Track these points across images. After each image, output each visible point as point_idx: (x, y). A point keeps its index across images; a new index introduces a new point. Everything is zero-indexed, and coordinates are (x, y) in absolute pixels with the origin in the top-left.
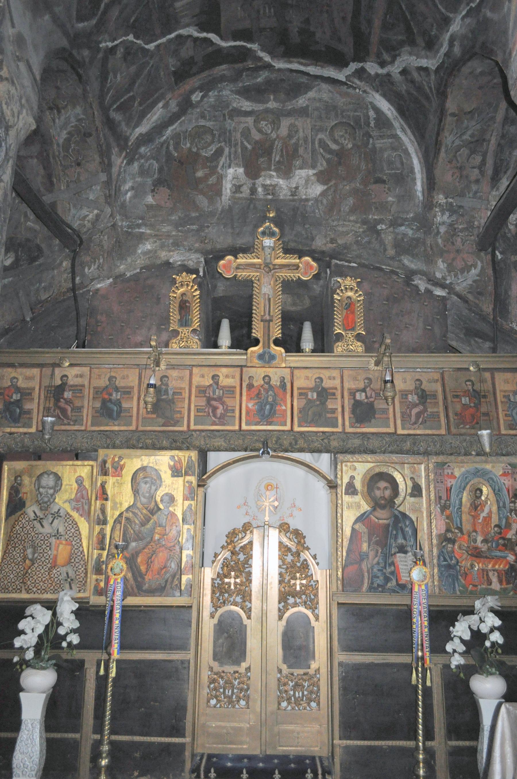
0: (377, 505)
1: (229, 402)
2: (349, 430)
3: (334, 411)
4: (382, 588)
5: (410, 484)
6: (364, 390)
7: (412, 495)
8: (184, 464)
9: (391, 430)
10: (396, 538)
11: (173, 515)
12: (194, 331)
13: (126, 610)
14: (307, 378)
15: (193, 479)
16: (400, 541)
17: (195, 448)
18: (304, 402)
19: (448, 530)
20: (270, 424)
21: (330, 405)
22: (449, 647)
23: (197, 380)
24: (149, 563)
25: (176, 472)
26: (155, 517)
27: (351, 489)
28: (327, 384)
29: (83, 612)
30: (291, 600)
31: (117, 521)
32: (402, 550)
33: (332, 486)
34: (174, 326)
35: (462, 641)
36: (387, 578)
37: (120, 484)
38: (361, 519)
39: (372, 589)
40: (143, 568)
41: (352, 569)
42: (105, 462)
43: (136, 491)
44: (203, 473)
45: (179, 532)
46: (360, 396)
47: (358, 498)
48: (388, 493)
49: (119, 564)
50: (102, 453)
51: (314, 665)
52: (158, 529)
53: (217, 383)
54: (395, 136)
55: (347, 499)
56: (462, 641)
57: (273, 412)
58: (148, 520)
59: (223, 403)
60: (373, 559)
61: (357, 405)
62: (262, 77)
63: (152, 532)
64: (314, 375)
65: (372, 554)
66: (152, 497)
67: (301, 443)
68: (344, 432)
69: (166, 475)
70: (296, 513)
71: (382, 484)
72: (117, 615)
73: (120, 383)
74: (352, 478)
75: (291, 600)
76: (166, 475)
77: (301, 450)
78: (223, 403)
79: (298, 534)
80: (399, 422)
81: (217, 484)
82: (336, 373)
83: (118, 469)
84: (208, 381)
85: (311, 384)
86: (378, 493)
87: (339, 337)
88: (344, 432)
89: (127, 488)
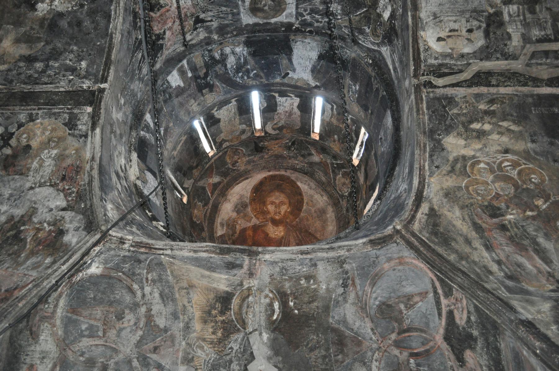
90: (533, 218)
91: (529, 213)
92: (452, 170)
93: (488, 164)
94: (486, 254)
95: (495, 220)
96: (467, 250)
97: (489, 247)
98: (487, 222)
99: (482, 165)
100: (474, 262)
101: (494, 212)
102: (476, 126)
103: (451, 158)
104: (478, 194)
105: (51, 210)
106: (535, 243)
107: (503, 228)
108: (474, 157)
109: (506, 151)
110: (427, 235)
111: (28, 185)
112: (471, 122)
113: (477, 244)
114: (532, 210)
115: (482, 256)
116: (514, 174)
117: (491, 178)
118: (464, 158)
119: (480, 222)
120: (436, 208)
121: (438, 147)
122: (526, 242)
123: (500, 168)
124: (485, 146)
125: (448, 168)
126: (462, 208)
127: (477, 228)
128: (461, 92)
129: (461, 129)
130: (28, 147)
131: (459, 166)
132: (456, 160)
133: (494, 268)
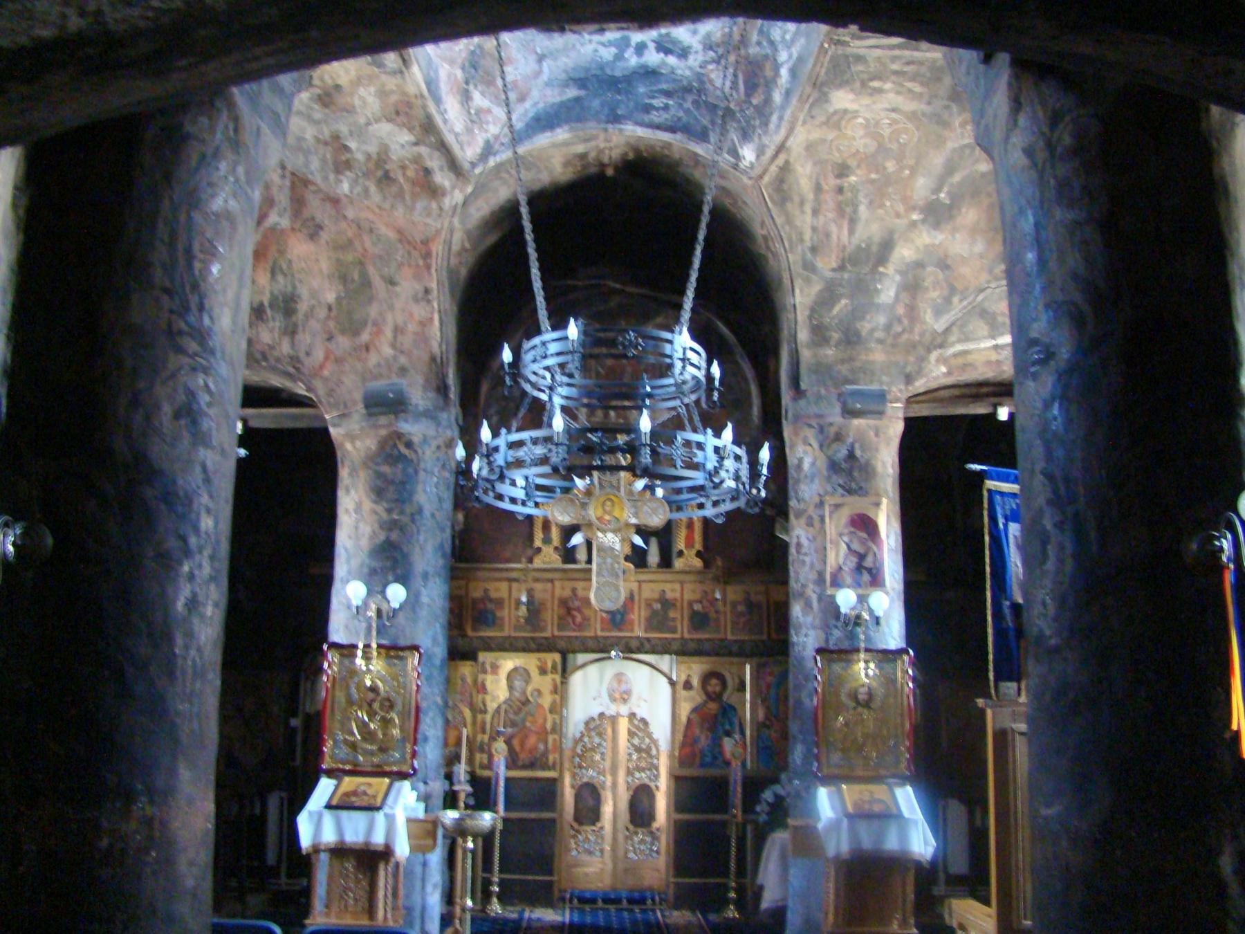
0: (710, 697)
2: (686, 636)
3: (674, 620)
4: (711, 765)
5: (737, 681)
7: (739, 690)
8: (549, 665)
9: (722, 636)
10: (723, 725)
11: (540, 706)
12: (556, 548)
13: (507, 780)
14: (652, 590)
15: (558, 678)
16: (727, 727)
17: (559, 651)
19: (767, 718)
20: (620, 630)
21: (672, 614)
22: (758, 808)
23: (558, 592)
24: (522, 744)
25: (543, 671)
26: (526, 709)
27: (688, 685)
28: (669, 595)
29: (474, 780)
31: (498, 710)
32: (728, 734)
33: (672, 683)
34: (538, 543)
35: (768, 804)
37: (497, 681)
38: (695, 710)
39: (702, 765)
40: (517, 748)
41: (687, 750)
42: (483, 663)
43: (511, 688)
44: (565, 671)
45: (545, 720)
46: (697, 607)
47: (692, 693)
48: (718, 689)
49: (500, 747)
50: (482, 656)
51: (655, 825)
52: (530, 718)
54: (736, 363)
55: (683, 693)
56: (768, 804)
57: (622, 620)
58: (520, 710)
60: (704, 741)
62: (613, 303)
63: (524, 721)
64: (658, 587)
65: (703, 739)
66: (524, 693)
67: (647, 646)
68: (682, 638)
69: (534, 673)
70: (642, 704)
71: (714, 681)
73: (493, 595)
77: (646, 653)
79: (644, 721)
81: (577, 679)
82: (677, 586)
83: (495, 668)
84: (567, 593)
85: (656, 596)
86: (710, 689)
87: (681, 553)
88: (682, 638)
89: (504, 682)
90: (872, 182)
91: (873, 176)
92: (826, 123)
93: (866, 119)
94: (808, 218)
95: (838, 181)
96: (797, 213)
97: (815, 212)
98: (831, 182)
99: (860, 120)
100: (796, 227)
101: (842, 171)
102: (875, 84)
103: (831, 110)
104: (839, 150)
105: (403, 146)
106: (855, 211)
107: (840, 190)
108: (857, 111)
109: (894, 110)
110: (770, 191)
111: (362, 121)
112: (871, 80)
113: (808, 209)
114: (877, 172)
115: (805, 221)
116: (886, 132)
117: (861, 132)
118: (845, 111)
119: (823, 183)
120: (792, 160)
121: (824, 98)
122: (848, 210)
123: (877, 124)
124: (874, 103)
125: (823, 119)
126: (815, 164)
127: (818, 189)
128: (878, 52)
129: (857, 85)
130: (338, 87)
131: (836, 118)
132: (836, 112)
133: (808, 235)
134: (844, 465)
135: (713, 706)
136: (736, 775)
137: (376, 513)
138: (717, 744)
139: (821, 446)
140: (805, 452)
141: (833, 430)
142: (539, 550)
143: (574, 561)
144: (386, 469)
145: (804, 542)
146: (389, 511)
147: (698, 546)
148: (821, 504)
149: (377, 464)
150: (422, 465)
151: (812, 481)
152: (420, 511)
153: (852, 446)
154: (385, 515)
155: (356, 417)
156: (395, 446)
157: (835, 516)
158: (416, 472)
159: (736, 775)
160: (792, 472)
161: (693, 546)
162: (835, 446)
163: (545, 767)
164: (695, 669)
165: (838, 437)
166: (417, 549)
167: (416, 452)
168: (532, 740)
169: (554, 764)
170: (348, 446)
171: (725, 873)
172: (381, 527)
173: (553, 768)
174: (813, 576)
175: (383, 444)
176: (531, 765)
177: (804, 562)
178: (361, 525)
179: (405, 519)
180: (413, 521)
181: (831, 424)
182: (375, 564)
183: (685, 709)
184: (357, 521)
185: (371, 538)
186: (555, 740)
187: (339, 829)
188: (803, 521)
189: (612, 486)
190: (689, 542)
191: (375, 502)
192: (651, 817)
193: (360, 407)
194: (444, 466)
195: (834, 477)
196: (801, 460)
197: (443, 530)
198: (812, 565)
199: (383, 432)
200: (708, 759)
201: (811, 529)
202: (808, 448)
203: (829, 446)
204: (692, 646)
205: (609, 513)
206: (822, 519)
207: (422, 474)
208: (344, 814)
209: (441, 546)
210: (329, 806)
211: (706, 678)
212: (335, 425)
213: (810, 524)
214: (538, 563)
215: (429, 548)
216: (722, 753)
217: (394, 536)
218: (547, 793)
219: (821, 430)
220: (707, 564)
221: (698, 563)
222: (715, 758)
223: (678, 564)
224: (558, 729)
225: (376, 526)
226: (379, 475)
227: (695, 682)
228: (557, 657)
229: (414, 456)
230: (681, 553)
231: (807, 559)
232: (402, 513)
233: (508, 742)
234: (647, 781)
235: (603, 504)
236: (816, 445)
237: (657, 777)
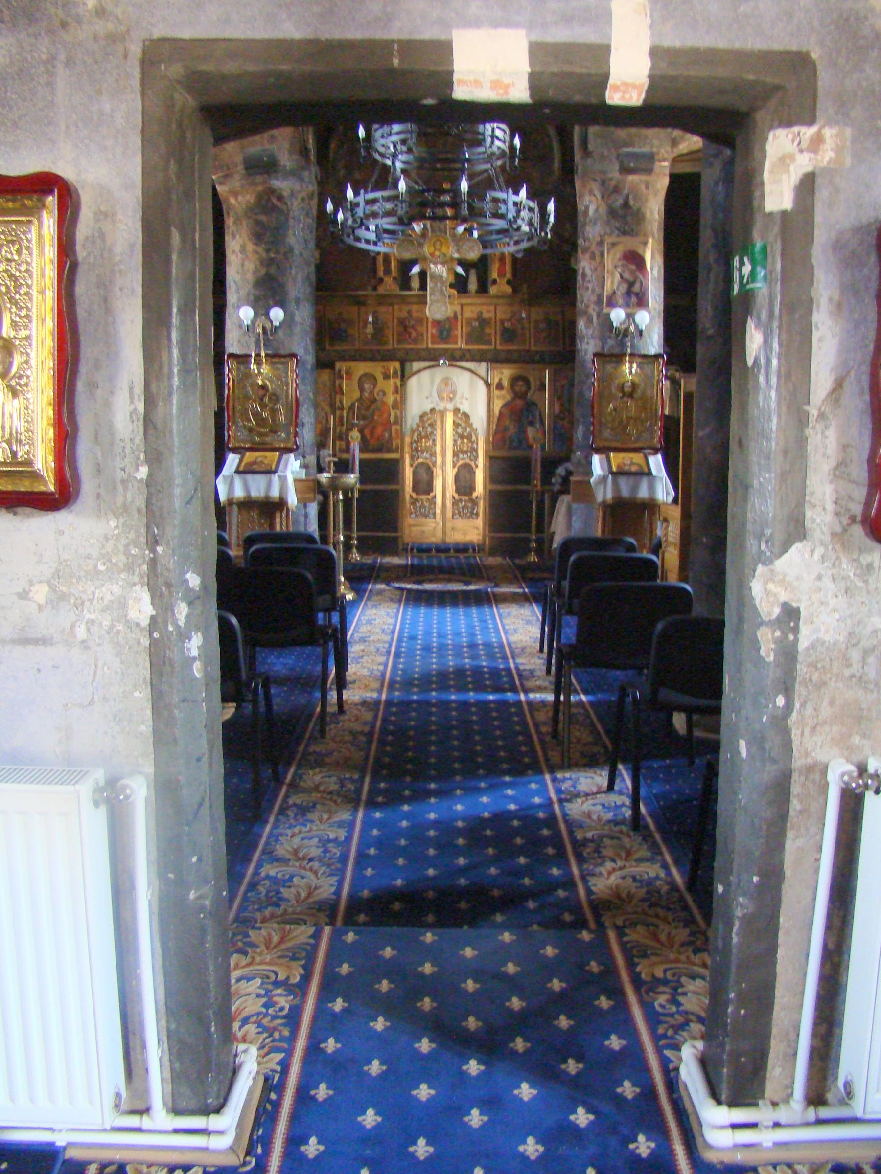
0: (516, 395)
1: (419, 329)
2: (499, 347)
3: (489, 334)
4: (515, 448)
5: (538, 383)
6: (510, 320)
9: (527, 348)
11: (384, 403)
12: (394, 278)
13: (361, 461)
17: (398, 360)
18: (469, 329)
19: (561, 412)
20: (447, 343)
21: (487, 331)
22: (553, 480)
23: (397, 314)
27: (500, 386)
28: (486, 315)
30: (461, 456)
31: (351, 408)
32: (531, 423)
33: (488, 385)
34: (381, 274)
36: (521, 441)
38: (505, 406)
40: (368, 437)
41: (499, 436)
42: (340, 371)
43: (362, 390)
44: (404, 377)
46: (507, 325)
47: (504, 392)
48: (523, 389)
49: (355, 435)
50: (338, 365)
51: (475, 495)
53: (411, 316)
55: (497, 393)
57: (448, 335)
58: (370, 407)
59: (416, 330)
60: (512, 430)
61: (505, 330)
63: (373, 414)
64: (476, 309)
65: (512, 427)
66: (371, 393)
67: (468, 356)
69: (380, 378)
70: (464, 401)
71: (520, 383)
72: (357, 463)
73: (345, 316)
74: (501, 380)
75: (461, 456)
76: (380, 378)
77: (467, 361)
78: (416, 330)
79: (466, 415)
80: (532, 341)
81: (413, 383)
82: (492, 308)
84: (404, 314)
85: (475, 316)
86: (517, 389)
87: (495, 282)
134: (620, 212)
135: (519, 403)
136: (537, 456)
137: (257, 253)
138: (522, 432)
139: (603, 197)
140: (590, 201)
141: (613, 183)
142: (381, 280)
143: (409, 289)
144: (263, 218)
145: (588, 272)
146: (268, 251)
147: (509, 276)
148: (601, 243)
149: (256, 214)
150: (291, 214)
151: (595, 224)
152: (291, 249)
153: (627, 196)
154: (264, 255)
155: (237, 177)
156: (269, 199)
157: (612, 252)
158: (287, 220)
159: (537, 456)
160: (580, 218)
161: (504, 275)
162: (613, 197)
163: (389, 450)
164: (505, 374)
165: (617, 190)
166: (290, 280)
167: (286, 204)
168: (380, 429)
169: (397, 448)
170: (232, 200)
171: (529, 530)
172: (262, 263)
173: (396, 450)
174: (594, 298)
175: (259, 197)
176: (379, 450)
177: (588, 288)
178: (246, 263)
179: (280, 257)
180: (287, 259)
181: (611, 179)
182: (258, 292)
183: (498, 405)
184: (243, 260)
185: (254, 273)
186: (397, 430)
187: (247, 488)
188: (587, 256)
189: (440, 230)
190: (502, 274)
191: (257, 244)
192: (472, 488)
193: (240, 168)
194: (307, 215)
195: (613, 221)
196: (587, 208)
197: (309, 265)
198: (593, 291)
199: (260, 188)
200: (515, 444)
201: (593, 263)
202: (593, 198)
203: (609, 196)
204: (503, 356)
205: (440, 250)
206: (602, 255)
207: (291, 222)
208: (249, 477)
209: (308, 278)
210: (237, 472)
211: (514, 380)
212: (221, 184)
213: (593, 257)
214: (381, 290)
215: (299, 278)
216: (527, 438)
217: (273, 270)
218: (392, 471)
219: (603, 183)
220: (515, 290)
221: (508, 289)
222: (520, 442)
223: (493, 290)
224: (399, 421)
225: (258, 263)
226: (258, 223)
227: (505, 383)
228: (397, 365)
229: (284, 207)
230: (495, 282)
231: (590, 286)
232: (277, 252)
233: (361, 431)
234: (468, 461)
235: (434, 245)
236: (599, 196)
237: (476, 458)
